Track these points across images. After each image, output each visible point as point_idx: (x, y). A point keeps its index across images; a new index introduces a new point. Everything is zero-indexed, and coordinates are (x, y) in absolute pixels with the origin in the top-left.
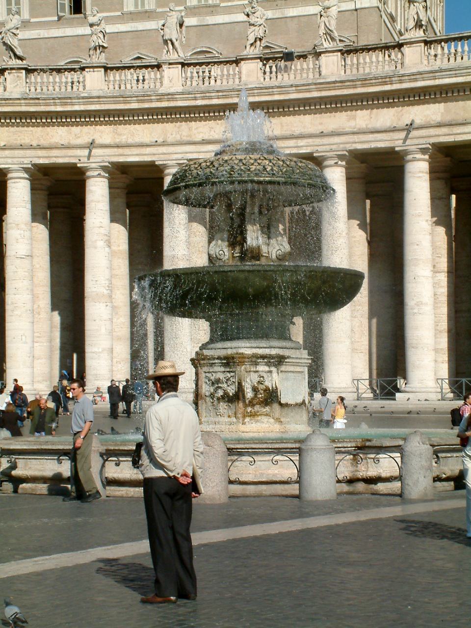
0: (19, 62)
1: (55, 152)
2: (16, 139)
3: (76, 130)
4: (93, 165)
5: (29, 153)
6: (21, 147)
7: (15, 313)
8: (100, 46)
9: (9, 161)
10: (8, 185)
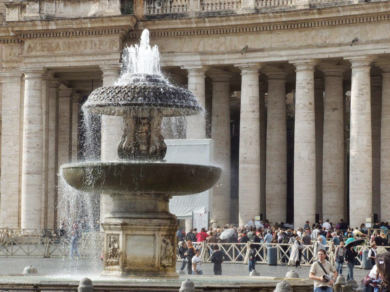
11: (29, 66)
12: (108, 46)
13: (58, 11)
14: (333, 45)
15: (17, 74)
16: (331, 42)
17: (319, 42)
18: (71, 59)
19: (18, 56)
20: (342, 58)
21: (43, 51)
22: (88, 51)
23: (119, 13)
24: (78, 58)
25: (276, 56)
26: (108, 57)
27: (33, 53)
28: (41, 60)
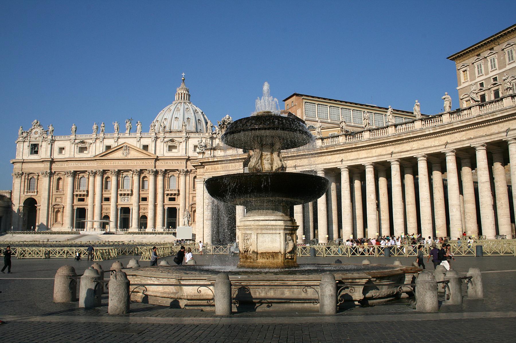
0: (476, 103)
1: (493, 137)
2: (477, 134)
3: (501, 125)
4: (510, 139)
5: (482, 139)
6: (480, 137)
7: (483, 206)
8: (508, 88)
9: (475, 143)
10: (476, 153)
11: (207, 176)
13: (218, 154)
14: (333, 162)
15: (202, 180)
16: (332, 161)
17: (327, 161)
20: (337, 167)
21: (212, 170)
22: (230, 169)
23: (243, 153)
25: (308, 168)
27: (208, 171)
28: (211, 173)
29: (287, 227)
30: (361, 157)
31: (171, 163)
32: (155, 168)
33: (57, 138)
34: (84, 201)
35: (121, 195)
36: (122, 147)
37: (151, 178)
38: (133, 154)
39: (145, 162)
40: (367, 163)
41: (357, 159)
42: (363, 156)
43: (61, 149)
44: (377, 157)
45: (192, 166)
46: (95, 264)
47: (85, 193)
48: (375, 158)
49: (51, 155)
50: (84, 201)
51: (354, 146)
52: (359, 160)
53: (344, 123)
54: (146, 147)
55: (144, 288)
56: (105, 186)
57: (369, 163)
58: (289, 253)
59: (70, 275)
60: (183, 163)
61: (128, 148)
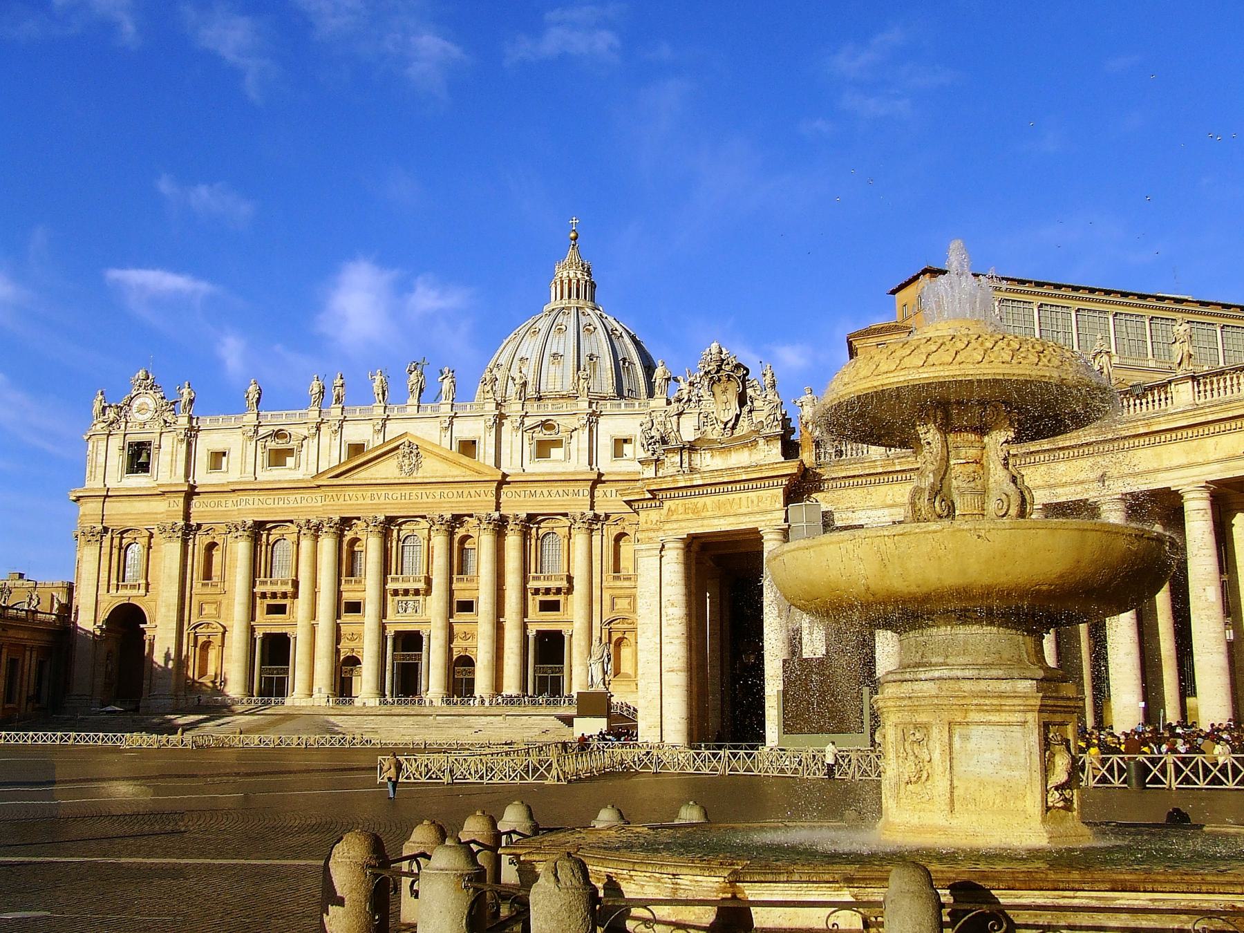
12: (769, 502)
13: (704, 465)
15: (655, 546)
18: (722, 521)
19: (656, 524)
22: (744, 510)
24: (732, 520)
26: (769, 516)
27: (674, 517)
28: (683, 524)
29: (1049, 702)
30: (1166, 464)
31: (546, 494)
32: (498, 508)
33: (205, 423)
34: (284, 613)
35: (396, 593)
36: (397, 448)
37: (484, 543)
38: (431, 468)
39: (554, 491)
40: (1188, 485)
41: (1157, 471)
42: (1175, 463)
43: (217, 458)
44: (1224, 464)
45: (624, 501)
46: (426, 822)
47: (289, 588)
48: (1216, 466)
49: (187, 475)
50: (284, 613)
51: (1142, 431)
52: (1160, 476)
53: (1106, 358)
54: (468, 447)
55: (647, 911)
56: (347, 564)
57: (1193, 482)
58: (1057, 788)
59: (373, 863)
60: (581, 494)
61: (412, 451)
